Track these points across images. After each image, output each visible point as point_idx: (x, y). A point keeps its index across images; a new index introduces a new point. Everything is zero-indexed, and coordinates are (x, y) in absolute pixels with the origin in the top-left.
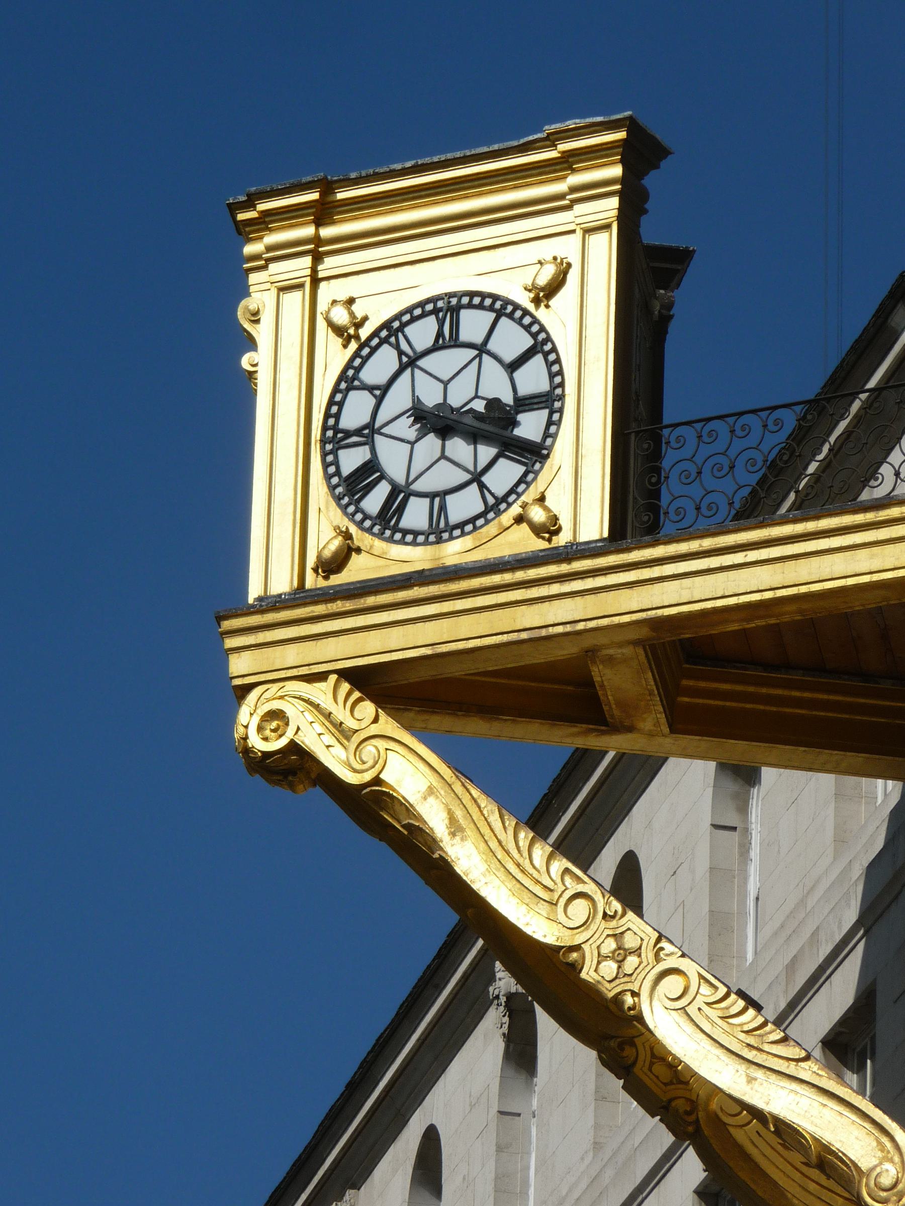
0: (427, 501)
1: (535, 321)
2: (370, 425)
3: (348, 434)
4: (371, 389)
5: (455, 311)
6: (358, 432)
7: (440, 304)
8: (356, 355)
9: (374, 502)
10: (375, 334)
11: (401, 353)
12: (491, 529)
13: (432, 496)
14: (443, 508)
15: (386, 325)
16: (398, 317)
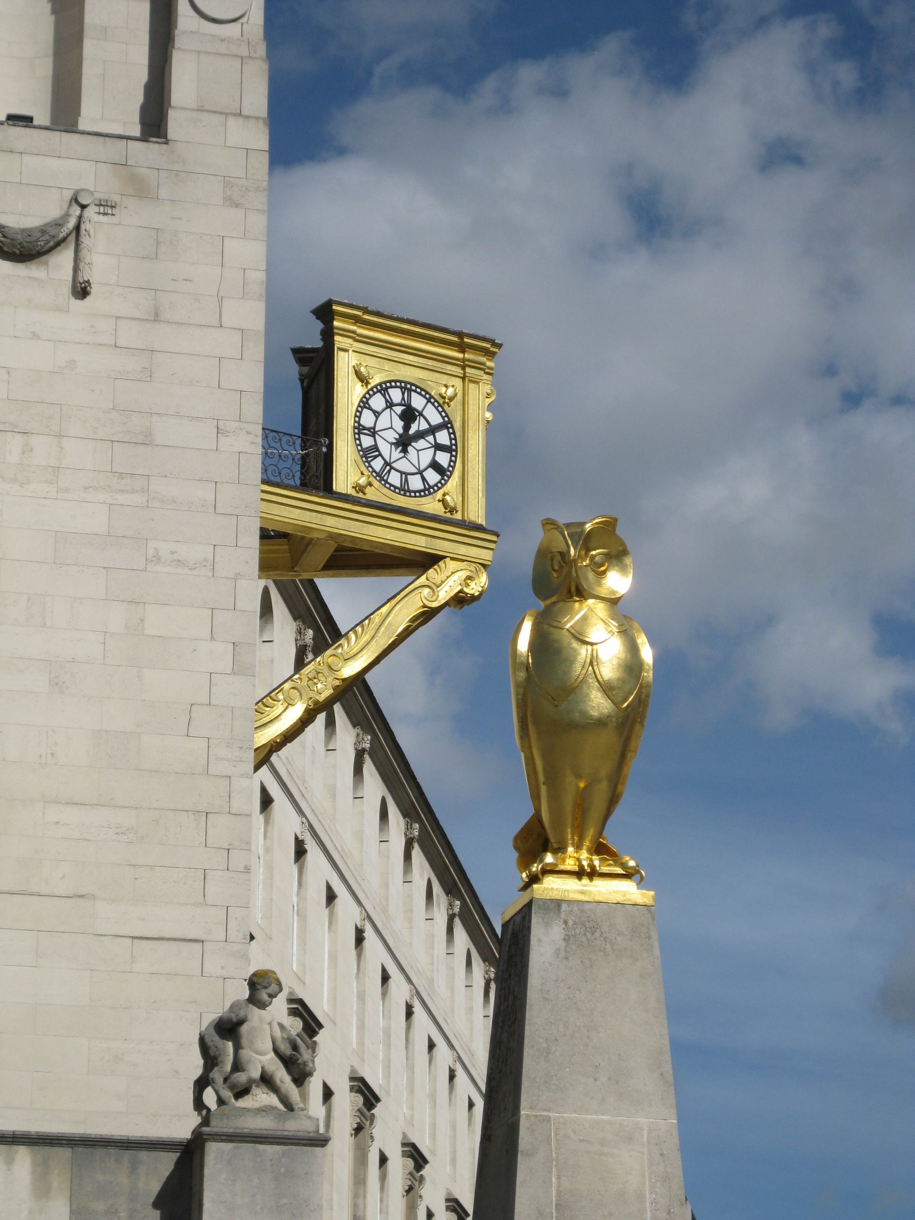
1: (444, 411)
3: (365, 428)
4: (374, 412)
5: (410, 390)
6: (369, 429)
7: (403, 384)
8: (368, 393)
9: (378, 464)
10: (376, 386)
11: (387, 401)
12: (428, 498)
13: (401, 473)
14: (406, 480)
15: (380, 384)
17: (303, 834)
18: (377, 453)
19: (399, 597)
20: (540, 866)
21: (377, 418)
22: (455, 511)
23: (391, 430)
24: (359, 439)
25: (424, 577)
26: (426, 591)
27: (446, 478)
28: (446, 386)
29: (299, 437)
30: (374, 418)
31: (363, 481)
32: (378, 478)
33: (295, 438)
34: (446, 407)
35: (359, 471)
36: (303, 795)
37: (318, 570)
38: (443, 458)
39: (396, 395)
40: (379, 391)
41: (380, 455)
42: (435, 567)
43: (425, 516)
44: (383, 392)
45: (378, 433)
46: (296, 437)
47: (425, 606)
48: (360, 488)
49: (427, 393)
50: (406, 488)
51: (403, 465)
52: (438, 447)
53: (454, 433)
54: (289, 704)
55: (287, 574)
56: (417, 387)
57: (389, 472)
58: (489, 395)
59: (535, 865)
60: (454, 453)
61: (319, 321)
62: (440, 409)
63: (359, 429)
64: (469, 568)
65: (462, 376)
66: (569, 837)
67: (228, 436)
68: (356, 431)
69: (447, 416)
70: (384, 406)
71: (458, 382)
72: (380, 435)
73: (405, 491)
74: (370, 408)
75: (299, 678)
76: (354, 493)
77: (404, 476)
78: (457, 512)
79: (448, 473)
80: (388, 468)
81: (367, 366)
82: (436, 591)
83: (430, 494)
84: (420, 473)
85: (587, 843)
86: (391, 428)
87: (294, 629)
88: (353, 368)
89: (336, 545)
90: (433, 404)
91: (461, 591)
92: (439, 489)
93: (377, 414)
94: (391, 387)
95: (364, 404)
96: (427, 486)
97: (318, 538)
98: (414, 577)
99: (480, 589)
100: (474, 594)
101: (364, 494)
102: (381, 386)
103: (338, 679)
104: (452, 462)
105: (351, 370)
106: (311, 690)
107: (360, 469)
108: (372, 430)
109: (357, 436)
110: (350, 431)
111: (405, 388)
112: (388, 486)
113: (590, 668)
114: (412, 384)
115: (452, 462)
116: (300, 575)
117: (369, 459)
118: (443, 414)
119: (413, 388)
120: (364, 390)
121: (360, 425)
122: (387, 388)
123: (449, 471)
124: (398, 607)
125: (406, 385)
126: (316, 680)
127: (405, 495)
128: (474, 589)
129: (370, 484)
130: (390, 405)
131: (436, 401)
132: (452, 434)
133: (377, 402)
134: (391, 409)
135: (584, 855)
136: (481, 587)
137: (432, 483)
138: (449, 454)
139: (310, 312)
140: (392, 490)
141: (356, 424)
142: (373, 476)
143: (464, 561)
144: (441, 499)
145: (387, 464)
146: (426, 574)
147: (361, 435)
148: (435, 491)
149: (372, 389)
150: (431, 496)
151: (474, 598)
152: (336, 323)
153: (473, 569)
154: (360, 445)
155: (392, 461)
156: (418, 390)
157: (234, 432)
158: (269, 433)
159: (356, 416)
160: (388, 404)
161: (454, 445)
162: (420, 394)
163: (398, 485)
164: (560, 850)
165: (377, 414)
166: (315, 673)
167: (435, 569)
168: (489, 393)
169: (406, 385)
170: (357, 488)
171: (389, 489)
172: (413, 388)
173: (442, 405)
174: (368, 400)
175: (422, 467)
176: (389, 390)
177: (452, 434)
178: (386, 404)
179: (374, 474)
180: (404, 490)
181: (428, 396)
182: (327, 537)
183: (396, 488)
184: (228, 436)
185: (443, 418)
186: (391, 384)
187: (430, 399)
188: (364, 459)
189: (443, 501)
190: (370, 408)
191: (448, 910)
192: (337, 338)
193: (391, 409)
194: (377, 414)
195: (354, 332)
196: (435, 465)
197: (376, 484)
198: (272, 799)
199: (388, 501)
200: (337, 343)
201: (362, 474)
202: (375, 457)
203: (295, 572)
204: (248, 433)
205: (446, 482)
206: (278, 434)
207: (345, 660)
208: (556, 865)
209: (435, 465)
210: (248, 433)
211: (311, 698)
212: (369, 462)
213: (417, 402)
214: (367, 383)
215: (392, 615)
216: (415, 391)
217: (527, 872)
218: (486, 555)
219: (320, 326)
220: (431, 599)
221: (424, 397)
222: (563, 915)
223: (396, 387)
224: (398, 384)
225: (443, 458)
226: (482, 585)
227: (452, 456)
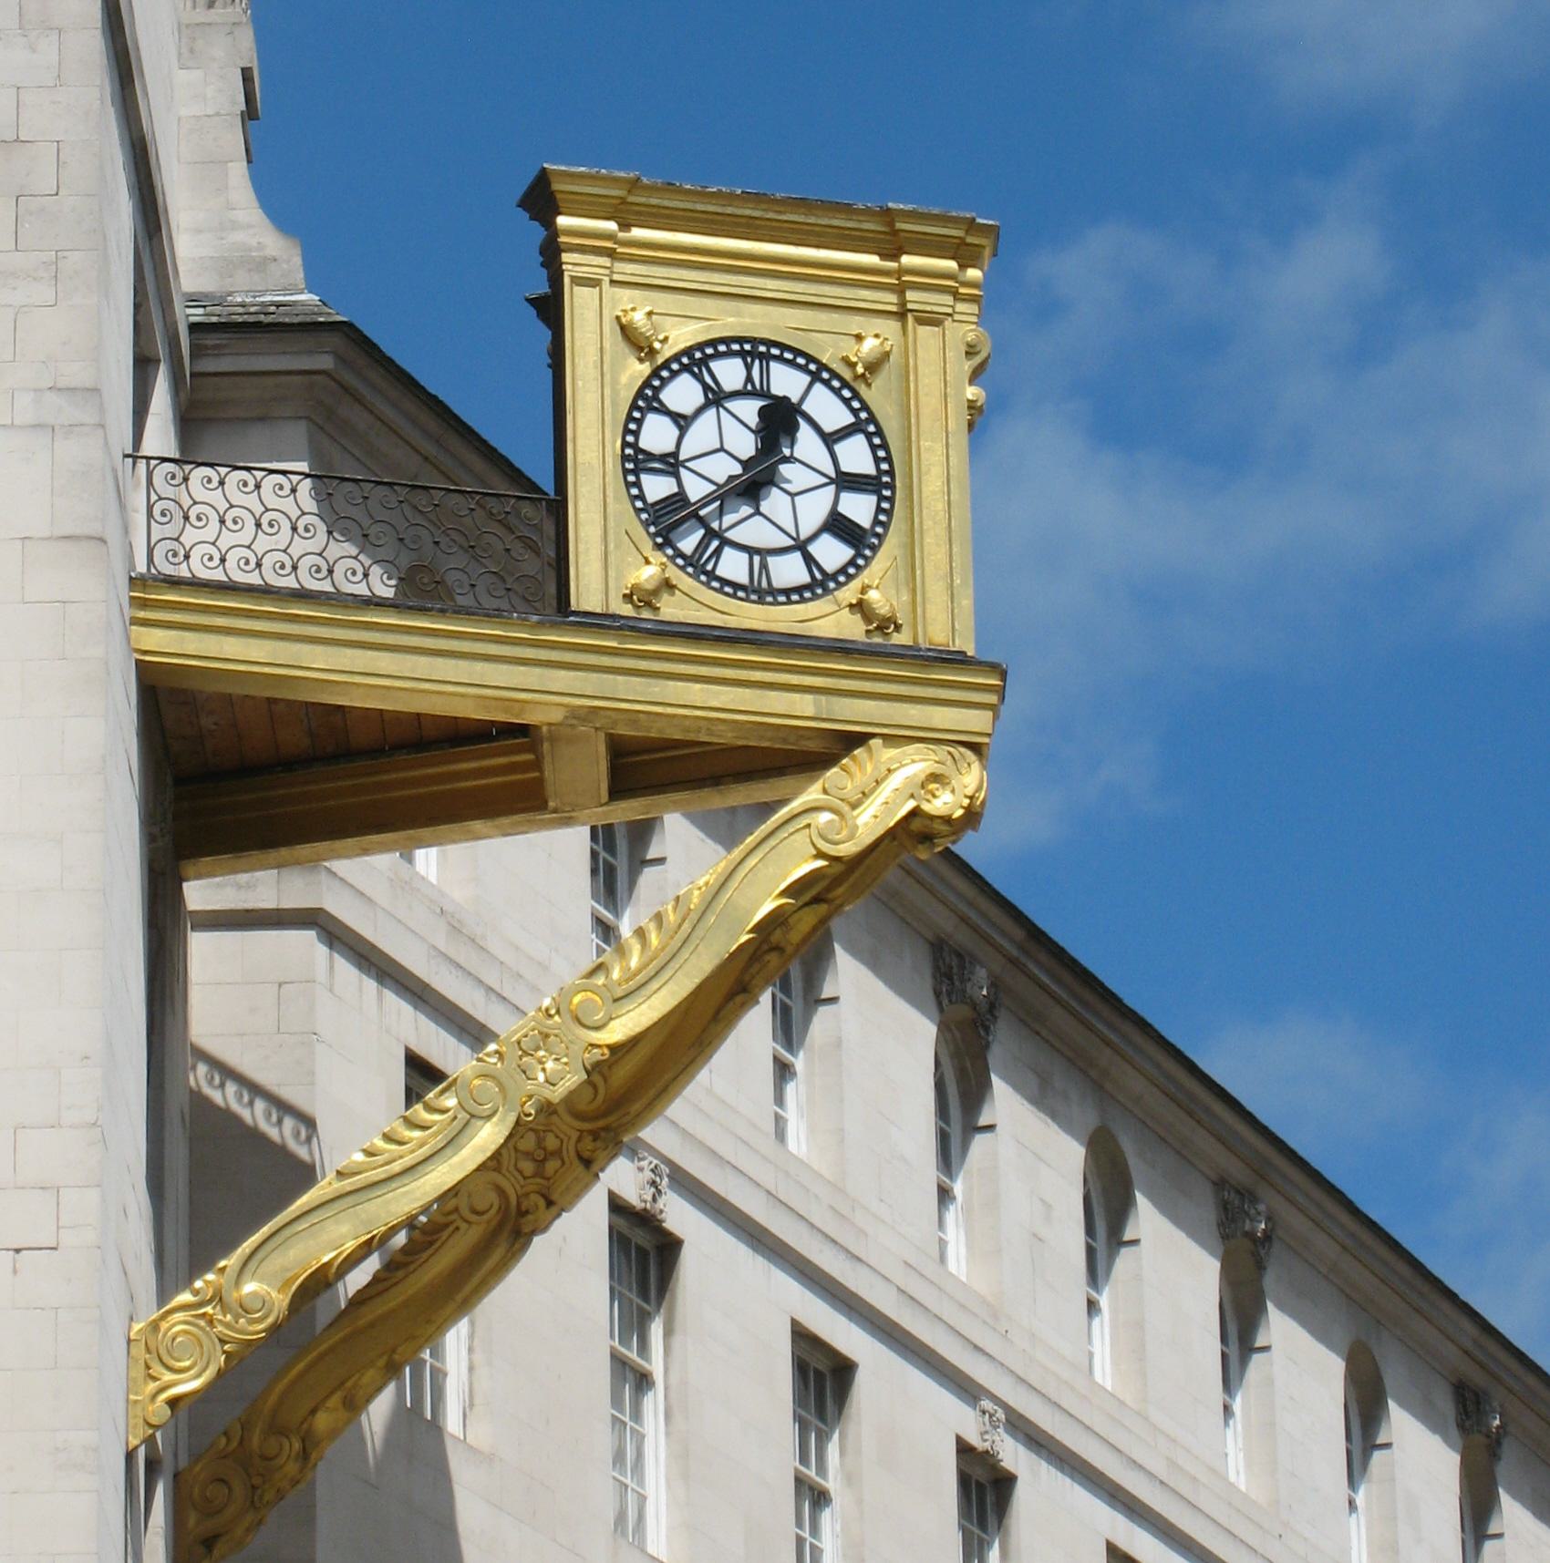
0: (745, 556)
1: (856, 395)
2: (675, 454)
3: (650, 456)
6: (662, 458)
8: (655, 373)
10: (676, 358)
11: (706, 388)
14: (764, 566)
15: (688, 352)
17: (986, 1437)
21: (683, 431)
22: (893, 626)
23: (722, 454)
24: (637, 484)
25: (818, 786)
26: (824, 817)
29: (307, 476)
30: (676, 432)
32: (690, 570)
33: (295, 478)
34: (862, 389)
35: (640, 557)
36: (976, 1347)
38: (859, 508)
39: (730, 373)
43: (806, 646)
44: (696, 370)
45: (687, 464)
46: (264, 473)
47: (820, 855)
48: (643, 597)
49: (810, 359)
50: (764, 584)
51: (754, 532)
52: (846, 482)
53: (884, 446)
54: (473, 1116)
55: (540, 820)
56: (784, 347)
57: (718, 552)
62: (847, 394)
63: (637, 461)
65: (894, 309)
69: (865, 407)
70: (700, 400)
71: (890, 327)
73: (758, 591)
75: (497, 1052)
76: (627, 610)
77: (757, 559)
78: (898, 628)
80: (715, 544)
82: (848, 817)
83: (827, 591)
84: (801, 546)
86: (722, 449)
88: (615, 322)
90: (827, 383)
91: (915, 813)
92: (850, 578)
93: (682, 423)
94: (718, 355)
95: (647, 400)
96: (818, 576)
97: (550, 724)
99: (966, 802)
100: (950, 816)
102: (691, 357)
103: (599, 1046)
104: (884, 514)
105: (610, 328)
106: (529, 1079)
107: (642, 554)
110: (609, 465)
112: (715, 584)
114: (771, 343)
115: (884, 514)
116: (571, 818)
120: (645, 369)
121: (638, 450)
122: (705, 360)
124: (752, 861)
127: (761, 601)
128: (944, 803)
129: (668, 585)
131: (835, 375)
132: (879, 445)
136: (966, 797)
137: (830, 564)
138: (874, 498)
140: (727, 594)
141: (629, 451)
144: (854, 601)
145: (711, 534)
146: (821, 781)
147: (644, 478)
148: (839, 585)
149: (666, 365)
150: (830, 597)
152: (562, 221)
154: (641, 497)
156: (722, 348)
158: (372, 489)
160: (710, 396)
162: (791, 363)
166: (539, 1037)
168: (972, 344)
170: (635, 597)
171: (720, 591)
173: (852, 384)
174: (657, 390)
175: (805, 533)
176: (713, 365)
177: (879, 445)
179: (680, 561)
180: (760, 592)
181: (812, 367)
182: (566, 717)
185: (855, 412)
186: (716, 349)
187: (818, 372)
189: (860, 607)
192: (565, 257)
194: (683, 422)
196: (838, 525)
197: (684, 580)
198: (853, 1361)
199: (716, 620)
200: (570, 267)
203: (555, 811)
206: (252, 474)
207: (616, 1000)
209: (838, 525)
211: (530, 1097)
213: (787, 381)
214: (652, 353)
215: (734, 883)
216: (780, 359)
218: (976, 721)
221: (804, 369)
223: (730, 354)
224: (736, 347)
225: (859, 508)
226: (969, 791)
227: (881, 498)
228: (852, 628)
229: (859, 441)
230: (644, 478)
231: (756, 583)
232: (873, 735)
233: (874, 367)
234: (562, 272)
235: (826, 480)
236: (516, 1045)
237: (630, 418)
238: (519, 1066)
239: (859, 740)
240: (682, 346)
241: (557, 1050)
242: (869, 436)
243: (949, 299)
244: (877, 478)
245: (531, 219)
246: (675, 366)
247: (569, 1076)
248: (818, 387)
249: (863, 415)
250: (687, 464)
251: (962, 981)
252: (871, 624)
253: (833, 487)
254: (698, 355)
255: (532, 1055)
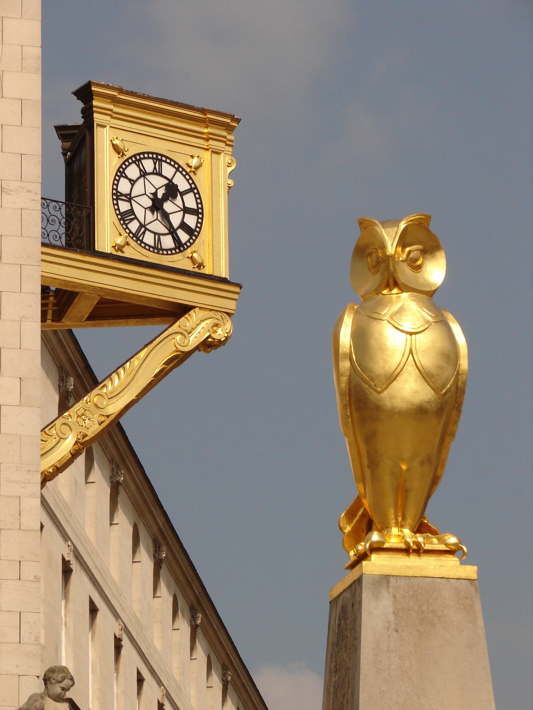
1: (191, 178)
3: (122, 195)
4: (130, 180)
5: (161, 160)
6: (125, 195)
8: (124, 163)
9: (134, 226)
10: (131, 158)
11: (140, 170)
13: (155, 234)
14: (159, 239)
15: (135, 156)
16: (139, 154)
18: (133, 217)
19: (155, 343)
20: (368, 545)
21: (133, 185)
22: (202, 267)
24: (117, 204)
26: (178, 337)
27: (194, 238)
28: (192, 157)
30: (130, 186)
31: (120, 241)
32: (134, 238)
34: (192, 174)
37: (82, 321)
38: (191, 220)
39: (148, 165)
40: (134, 162)
41: (136, 218)
42: (186, 316)
44: (137, 163)
45: (134, 199)
48: (120, 248)
49: (176, 163)
50: (159, 247)
52: (186, 210)
56: (167, 157)
57: (144, 233)
58: (229, 164)
59: (363, 543)
60: (200, 216)
61: (80, 101)
62: (187, 177)
63: (117, 196)
64: (215, 317)
66: (393, 516)
67: (11, 194)
68: (115, 197)
69: (194, 183)
70: (139, 175)
72: (135, 200)
74: (126, 177)
75: (69, 415)
76: (114, 253)
77: (157, 236)
78: (204, 267)
79: (196, 233)
80: (143, 229)
81: (123, 140)
85: (409, 521)
87: (57, 378)
89: (99, 298)
90: (181, 173)
93: (132, 182)
94: (144, 158)
95: (121, 173)
98: (167, 326)
100: (220, 339)
101: (123, 252)
102: (136, 158)
108: (129, 197)
109: (115, 202)
111: (157, 159)
112: (143, 245)
113: (411, 356)
114: (162, 155)
117: (126, 222)
118: (191, 182)
119: (164, 159)
121: (117, 192)
122: (140, 159)
123: (197, 231)
125: (157, 156)
126: (83, 417)
127: (158, 253)
128: (220, 334)
129: (128, 244)
130: (144, 174)
131: (183, 170)
132: (198, 199)
133: (133, 171)
134: (144, 177)
135: (407, 532)
136: (226, 333)
138: (196, 217)
139: (72, 93)
140: (147, 249)
141: (114, 192)
142: (130, 236)
143: (211, 310)
145: (141, 226)
146: (178, 322)
147: (119, 202)
149: (127, 160)
151: (220, 343)
152: (95, 103)
153: (220, 317)
154: (119, 209)
155: (146, 224)
157: (16, 191)
159: (114, 184)
160: (142, 173)
161: (200, 208)
162: (170, 164)
163: (152, 244)
164: (384, 528)
165: (132, 182)
167: (186, 318)
169: (157, 156)
170: (116, 247)
171: (145, 248)
172: (164, 159)
174: (124, 169)
176: (142, 161)
178: (140, 173)
180: (157, 249)
183: (150, 246)
184: (11, 194)
185: (190, 185)
187: (178, 168)
188: (122, 222)
190: (126, 177)
191: (191, 621)
192: (95, 115)
193: (144, 177)
194: (133, 182)
195: (111, 110)
201: (121, 235)
202: (132, 220)
204: (29, 191)
205: (194, 241)
207: (109, 399)
208: (383, 543)
210: (29, 191)
212: (126, 225)
214: (123, 155)
216: (166, 162)
217: (355, 550)
218: (231, 305)
219: (81, 105)
220: (183, 345)
221: (174, 166)
222: (391, 590)
224: (150, 156)
225: (191, 220)
227: (198, 218)
228: (188, 266)
229: (191, 194)
230: (119, 202)
231: (156, 246)
232: (195, 307)
233: (197, 168)
234: (94, 121)
235: (180, 209)
236: (76, 413)
237: (115, 179)
238: (77, 421)
239: (192, 308)
240: (132, 154)
241: (89, 416)
242: (195, 194)
243: (223, 145)
244: (197, 210)
245: (77, 99)
246: (130, 161)
247: (93, 426)
248: (178, 173)
249: (193, 186)
250: (134, 199)
251: (66, 382)
252: (195, 265)
253: (182, 212)
254: (138, 157)
255: (81, 417)
